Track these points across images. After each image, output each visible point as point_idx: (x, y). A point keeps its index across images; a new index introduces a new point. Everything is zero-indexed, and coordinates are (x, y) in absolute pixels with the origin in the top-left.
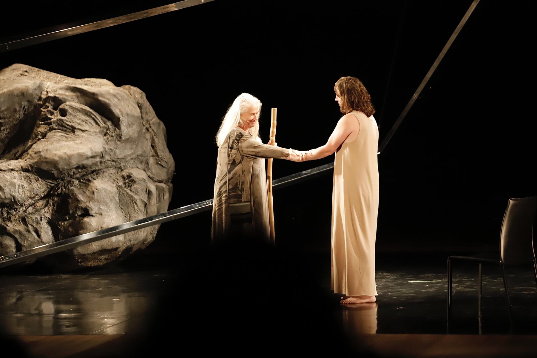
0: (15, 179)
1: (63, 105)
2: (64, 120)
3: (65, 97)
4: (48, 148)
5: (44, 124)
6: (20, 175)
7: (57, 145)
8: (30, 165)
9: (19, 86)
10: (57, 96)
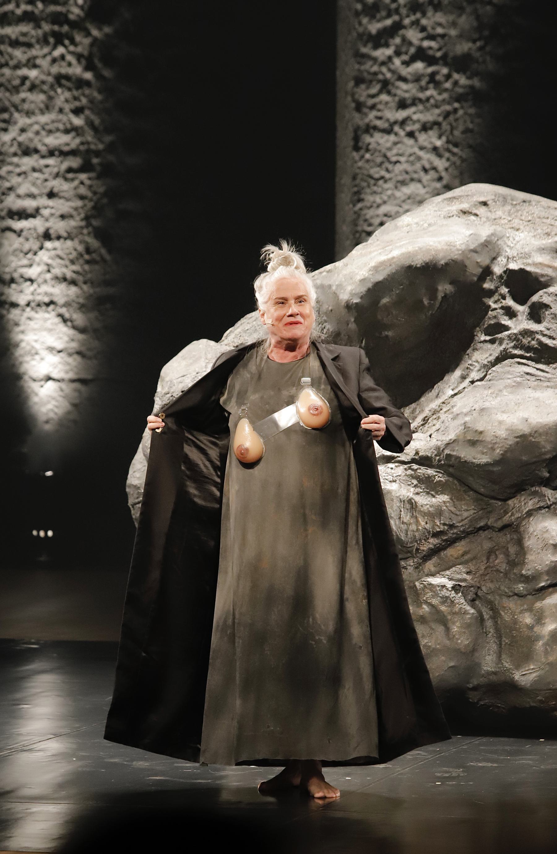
0: (394, 484)
1: (541, 292)
2: (537, 333)
3: (550, 272)
4: (487, 404)
5: (492, 342)
6: (410, 472)
7: (508, 397)
8: (438, 448)
9: (431, 243)
10: (528, 269)
